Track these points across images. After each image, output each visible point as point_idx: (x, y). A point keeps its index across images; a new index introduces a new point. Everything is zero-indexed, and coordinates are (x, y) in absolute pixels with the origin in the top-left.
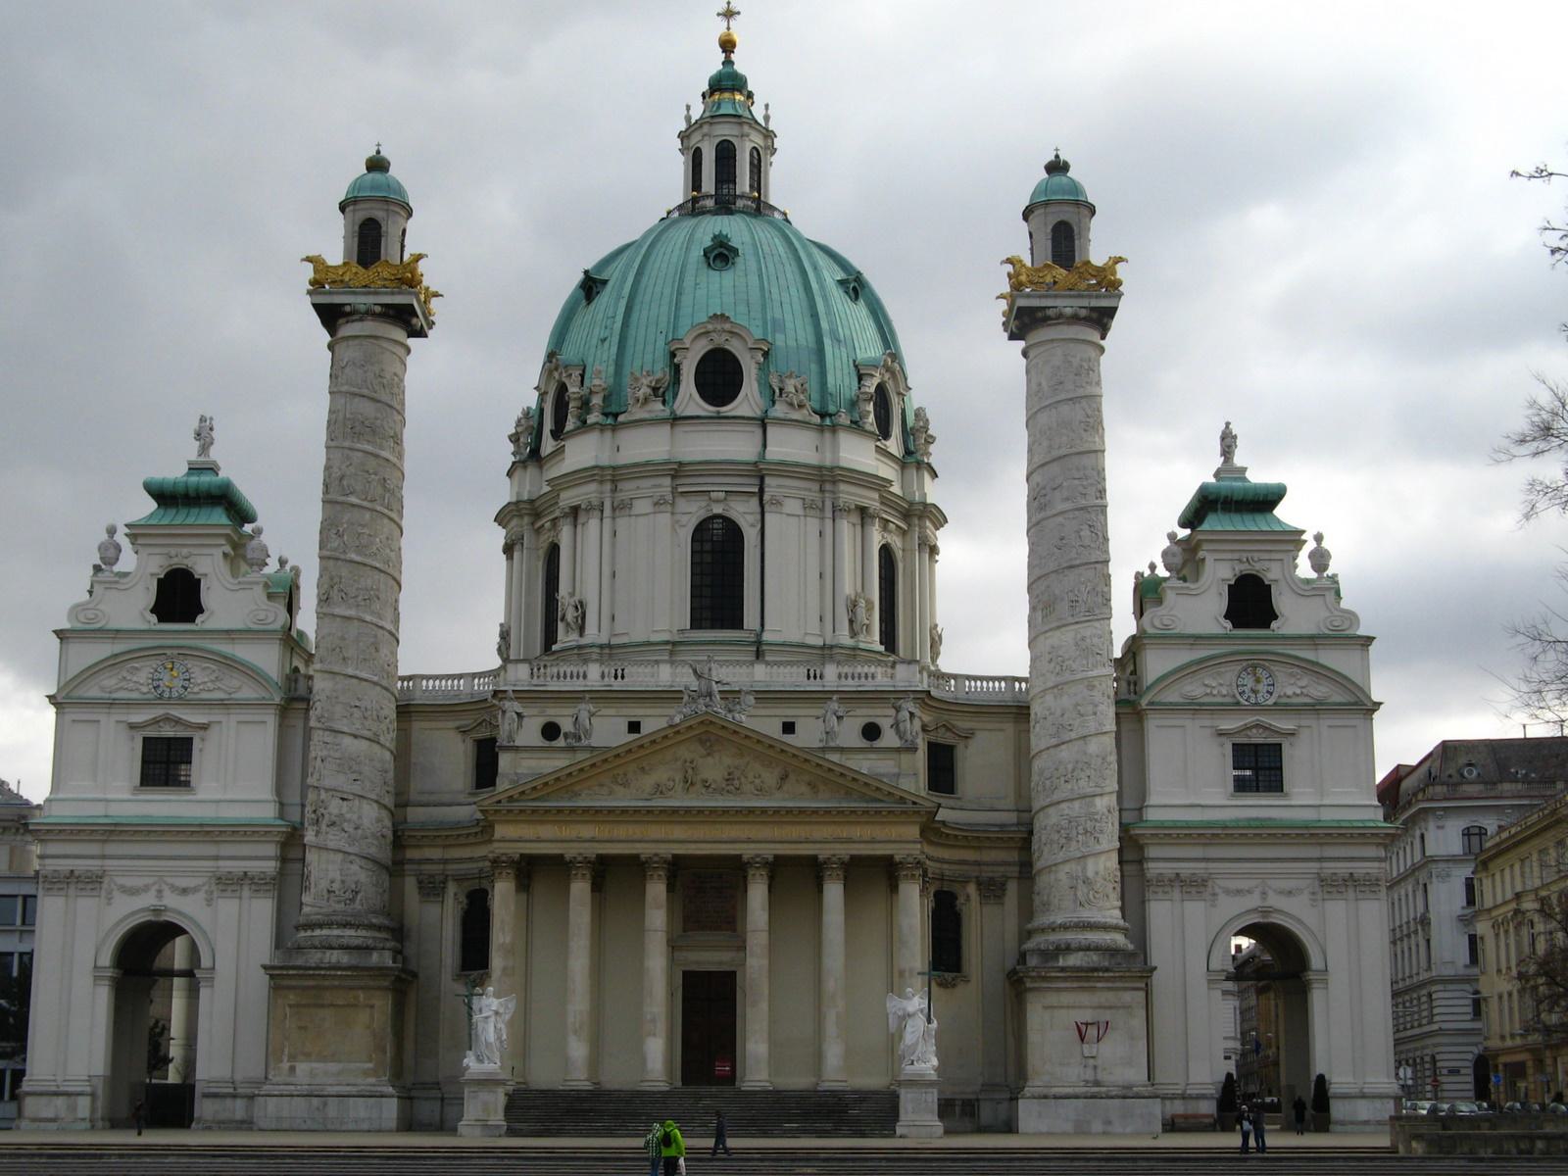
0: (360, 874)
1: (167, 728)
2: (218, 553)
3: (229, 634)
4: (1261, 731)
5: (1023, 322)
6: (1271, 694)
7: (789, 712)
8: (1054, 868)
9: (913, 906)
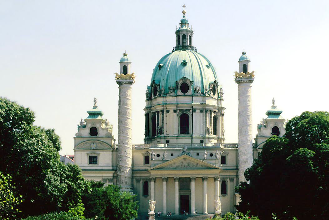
5: (238, 82)
7: (198, 152)
9: (218, 184)
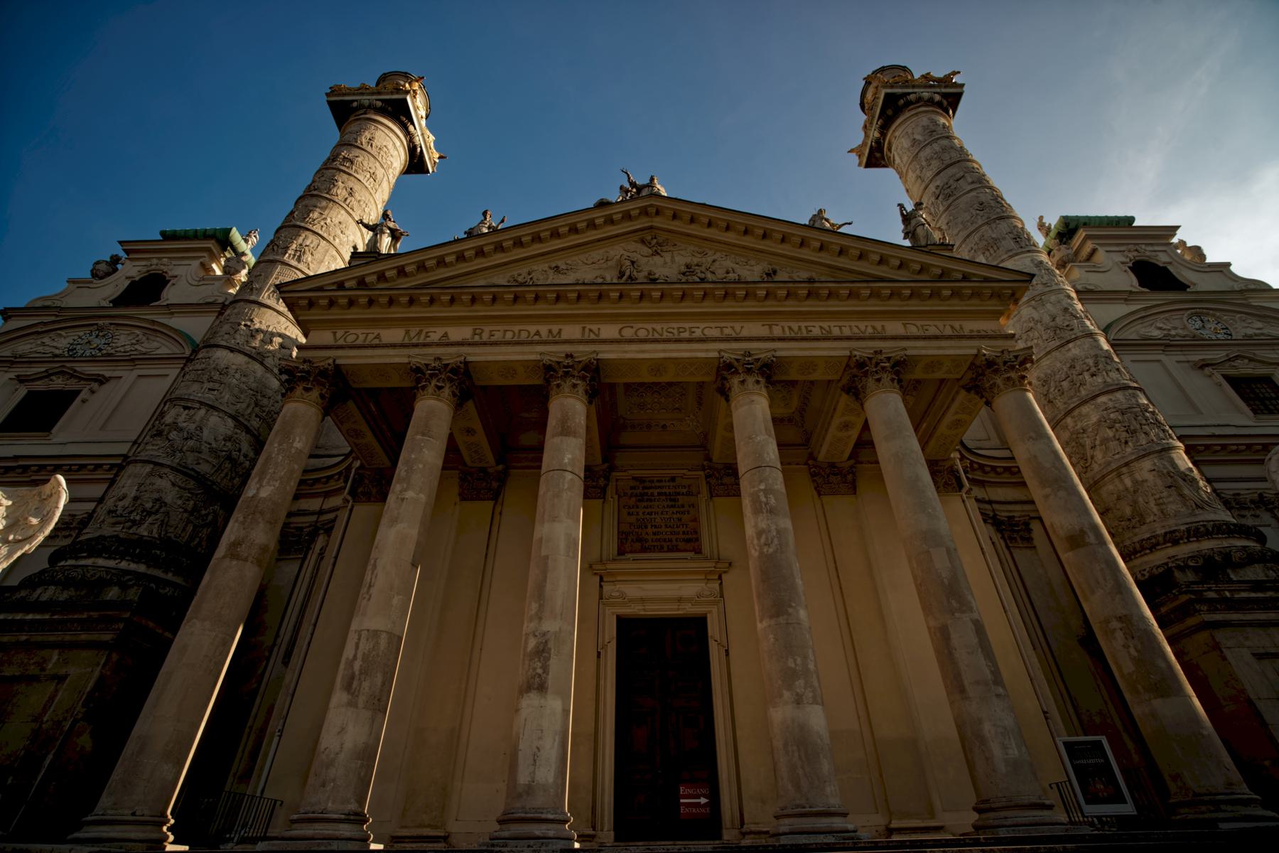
0: (167, 488)
1: (60, 381)
2: (196, 263)
3: (171, 309)
4: (1246, 361)
6: (1231, 335)
8: (1124, 470)
